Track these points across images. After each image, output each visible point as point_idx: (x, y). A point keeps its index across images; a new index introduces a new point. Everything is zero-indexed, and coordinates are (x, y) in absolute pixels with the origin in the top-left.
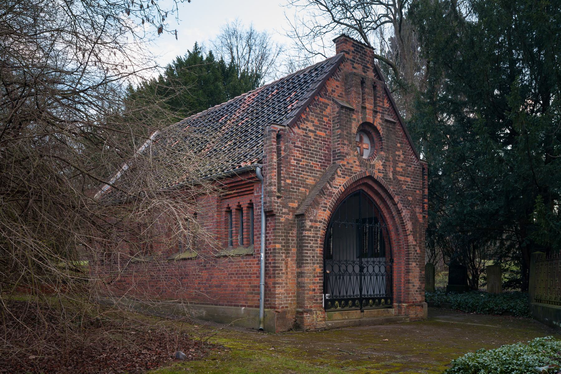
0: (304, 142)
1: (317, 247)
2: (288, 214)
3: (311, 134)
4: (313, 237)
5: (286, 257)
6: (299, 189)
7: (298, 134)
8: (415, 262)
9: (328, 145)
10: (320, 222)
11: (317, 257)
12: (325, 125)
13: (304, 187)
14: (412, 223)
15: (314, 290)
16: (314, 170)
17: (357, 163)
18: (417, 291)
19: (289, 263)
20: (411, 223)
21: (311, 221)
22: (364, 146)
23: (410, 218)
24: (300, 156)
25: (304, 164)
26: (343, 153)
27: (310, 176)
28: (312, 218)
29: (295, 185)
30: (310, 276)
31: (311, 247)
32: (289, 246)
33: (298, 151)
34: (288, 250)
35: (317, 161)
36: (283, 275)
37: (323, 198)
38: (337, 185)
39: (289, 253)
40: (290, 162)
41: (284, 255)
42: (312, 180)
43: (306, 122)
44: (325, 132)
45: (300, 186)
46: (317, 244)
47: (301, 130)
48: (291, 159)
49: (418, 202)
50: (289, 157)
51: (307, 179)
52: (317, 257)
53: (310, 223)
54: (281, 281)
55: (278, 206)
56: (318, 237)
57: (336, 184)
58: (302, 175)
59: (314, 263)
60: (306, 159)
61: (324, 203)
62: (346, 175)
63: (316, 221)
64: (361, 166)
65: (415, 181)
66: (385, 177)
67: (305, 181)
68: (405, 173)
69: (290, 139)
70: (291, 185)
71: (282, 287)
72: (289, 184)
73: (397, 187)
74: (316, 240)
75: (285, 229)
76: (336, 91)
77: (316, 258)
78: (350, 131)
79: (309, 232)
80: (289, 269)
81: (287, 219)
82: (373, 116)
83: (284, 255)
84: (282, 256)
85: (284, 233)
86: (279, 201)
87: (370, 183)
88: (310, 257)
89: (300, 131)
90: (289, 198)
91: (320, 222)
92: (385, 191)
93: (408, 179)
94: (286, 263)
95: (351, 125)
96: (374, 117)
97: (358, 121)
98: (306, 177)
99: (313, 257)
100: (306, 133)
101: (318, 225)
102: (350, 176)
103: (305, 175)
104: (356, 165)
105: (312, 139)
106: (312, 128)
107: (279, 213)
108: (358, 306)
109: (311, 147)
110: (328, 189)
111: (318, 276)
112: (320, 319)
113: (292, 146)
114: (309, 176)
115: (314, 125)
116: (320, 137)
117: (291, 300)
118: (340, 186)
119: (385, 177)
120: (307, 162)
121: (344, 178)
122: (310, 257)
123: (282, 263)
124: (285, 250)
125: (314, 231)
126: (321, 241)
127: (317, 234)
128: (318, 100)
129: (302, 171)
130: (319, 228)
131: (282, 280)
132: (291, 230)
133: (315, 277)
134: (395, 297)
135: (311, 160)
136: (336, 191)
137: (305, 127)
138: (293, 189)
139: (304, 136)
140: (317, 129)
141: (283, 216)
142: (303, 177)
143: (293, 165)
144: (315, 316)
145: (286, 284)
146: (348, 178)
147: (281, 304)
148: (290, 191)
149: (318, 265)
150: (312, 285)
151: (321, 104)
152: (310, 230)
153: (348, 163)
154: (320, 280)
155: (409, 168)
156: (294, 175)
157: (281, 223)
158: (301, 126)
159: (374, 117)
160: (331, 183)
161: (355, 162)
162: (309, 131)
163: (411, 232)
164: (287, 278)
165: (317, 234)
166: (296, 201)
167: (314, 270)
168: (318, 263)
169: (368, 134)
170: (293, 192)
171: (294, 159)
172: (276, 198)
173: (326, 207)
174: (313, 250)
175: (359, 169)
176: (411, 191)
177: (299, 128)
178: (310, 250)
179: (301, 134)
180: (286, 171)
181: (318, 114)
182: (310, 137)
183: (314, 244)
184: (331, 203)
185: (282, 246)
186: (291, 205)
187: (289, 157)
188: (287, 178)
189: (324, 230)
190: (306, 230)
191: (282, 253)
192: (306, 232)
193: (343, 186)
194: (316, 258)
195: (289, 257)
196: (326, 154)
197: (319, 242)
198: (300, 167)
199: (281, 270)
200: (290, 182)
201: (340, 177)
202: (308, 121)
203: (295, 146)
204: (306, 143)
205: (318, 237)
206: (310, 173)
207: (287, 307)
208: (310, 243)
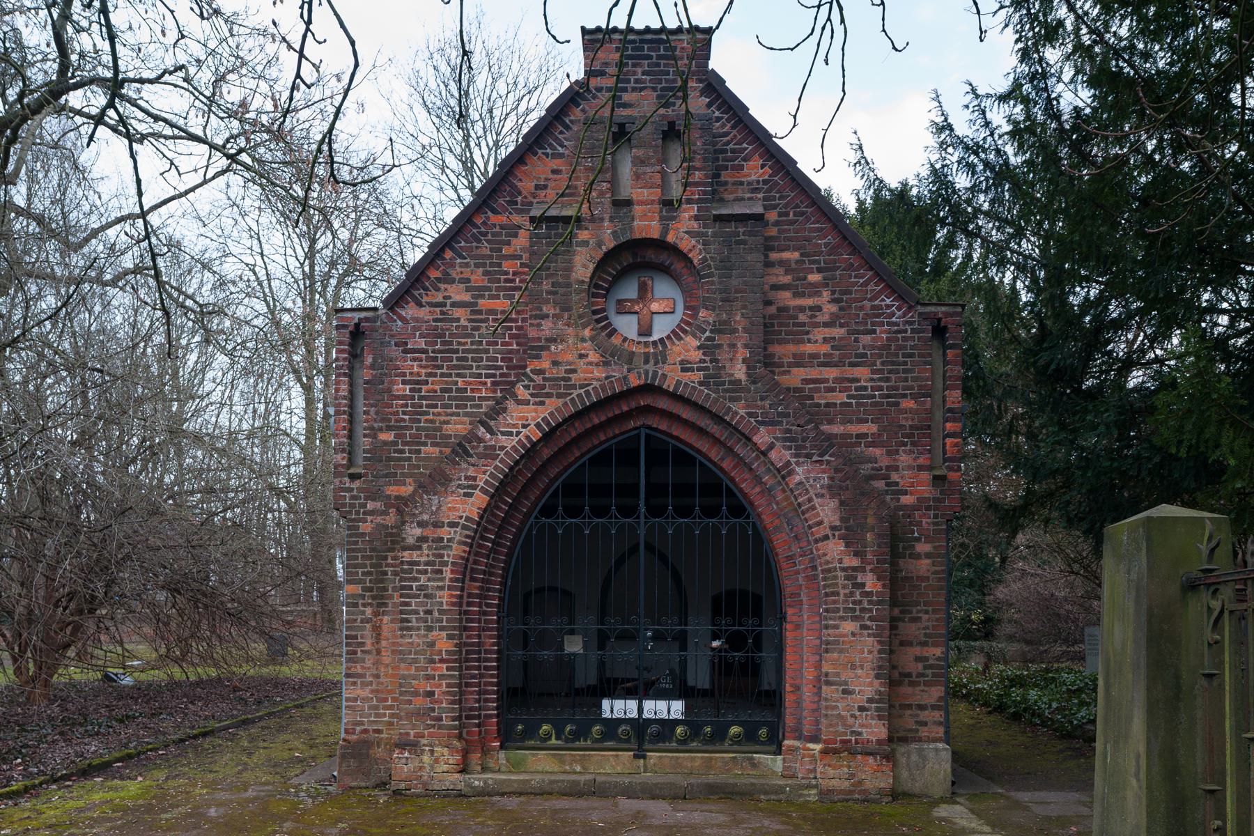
0: (435, 335)
1: (442, 588)
2: (385, 513)
3: (459, 313)
4: (427, 564)
5: (376, 614)
6: (419, 452)
7: (417, 320)
8: (854, 619)
9: (518, 328)
10: (453, 525)
11: (441, 612)
12: (506, 281)
13: (433, 445)
14: (842, 503)
15: (431, 694)
16: (473, 399)
17: (593, 357)
18: (861, 709)
19: (385, 628)
20: (834, 503)
21: (421, 524)
22: (655, 307)
23: (830, 487)
24: (423, 371)
25: (437, 387)
26: (539, 339)
27: (458, 415)
28: (426, 517)
29: (405, 444)
30: (415, 661)
31: (420, 588)
32: (385, 589)
33: (414, 359)
34: (382, 597)
35: (480, 375)
36: (367, 657)
37: (464, 465)
38: (515, 426)
39: (385, 605)
40: (389, 390)
41: (369, 611)
42: (462, 423)
43: (442, 286)
44: (511, 297)
45: (425, 444)
46: (443, 579)
47: (428, 309)
48: (395, 383)
49: (911, 436)
50: (387, 380)
51: (447, 422)
52: (441, 612)
53: (418, 532)
54: (359, 671)
55: (353, 498)
56: (445, 564)
57: (508, 425)
58: (431, 417)
59: (430, 629)
60: (442, 375)
61: (467, 478)
62: (549, 395)
63: (437, 525)
64: (606, 364)
65: (890, 372)
66: (714, 377)
67: (440, 429)
68: (842, 357)
69: (392, 336)
70: (395, 443)
71: (364, 684)
72: (385, 443)
73: (767, 403)
74: (441, 572)
75: (372, 550)
76: (551, 184)
77: (436, 614)
78: (568, 277)
79: (415, 553)
80: (384, 643)
81: (378, 524)
82: (662, 219)
83: (369, 611)
84: (363, 613)
85: (371, 558)
86: (357, 484)
87: (663, 404)
88: (417, 612)
89: (424, 313)
90: (387, 476)
91: (453, 525)
92: (718, 419)
93: (862, 373)
94: (377, 629)
95: (571, 261)
96: (666, 221)
97: (600, 244)
98: (443, 418)
99: (429, 612)
100: (442, 313)
101: (446, 533)
102: (559, 396)
103: (439, 414)
104: (591, 363)
105: (463, 322)
106: (467, 297)
107: (358, 513)
108: (628, 741)
109: (459, 344)
110: (480, 440)
111: (442, 661)
112: (445, 767)
113: (395, 352)
114: (452, 414)
115: (468, 289)
116: (491, 312)
117: (392, 716)
118: (525, 426)
119: (714, 377)
120: (447, 383)
121: (542, 403)
122: (417, 612)
123: (364, 629)
124: (374, 598)
125: (430, 548)
126: (452, 572)
127: (442, 556)
128: (484, 223)
129: (427, 406)
130: (449, 540)
131: (363, 668)
132: (392, 550)
133: (432, 661)
134: (789, 721)
135: (458, 375)
136: (509, 443)
137: (440, 299)
138: (402, 452)
139: (436, 320)
140: (483, 297)
141: (369, 518)
142: (432, 421)
143: (398, 398)
144: (426, 758)
145: (377, 676)
146: (552, 404)
147: (362, 723)
148: (390, 459)
149: (444, 634)
150: (423, 682)
151: (497, 229)
152: (420, 548)
153: (555, 363)
154: (448, 669)
155: (866, 339)
156: (404, 420)
157: (363, 535)
158: (425, 300)
159: (666, 221)
160: (492, 423)
161: (581, 356)
162: (454, 305)
163: (833, 528)
164: (377, 663)
165: (442, 556)
166: (408, 480)
167: (432, 644)
168: (442, 629)
169: (665, 270)
170: (399, 459)
171: (404, 382)
172: (346, 479)
173: (475, 487)
174: (426, 596)
175: (599, 373)
176: (875, 404)
177: (420, 305)
178: (418, 596)
179: (426, 318)
180: (377, 413)
181: (483, 257)
182: (458, 320)
183: (429, 580)
184: (492, 475)
185: (364, 589)
186: (392, 491)
187: (387, 380)
188: (381, 429)
189: (465, 544)
190: (405, 548)
191: (364, 605)
192: (406, 553)
193: (538, 425)
194: (436, 614)
195: (384, 613)
196: (511, 352)
197: (447, 573)
198: (421, 398)
199: (363, 644)
200: (392, 438)
201: (527, 403)
202: (452, 281)
203: (406, 351)
204: (442, 336)
205: (445, 564)
206: (457, 407)
207: (378, 731)
208: (416, 579)
